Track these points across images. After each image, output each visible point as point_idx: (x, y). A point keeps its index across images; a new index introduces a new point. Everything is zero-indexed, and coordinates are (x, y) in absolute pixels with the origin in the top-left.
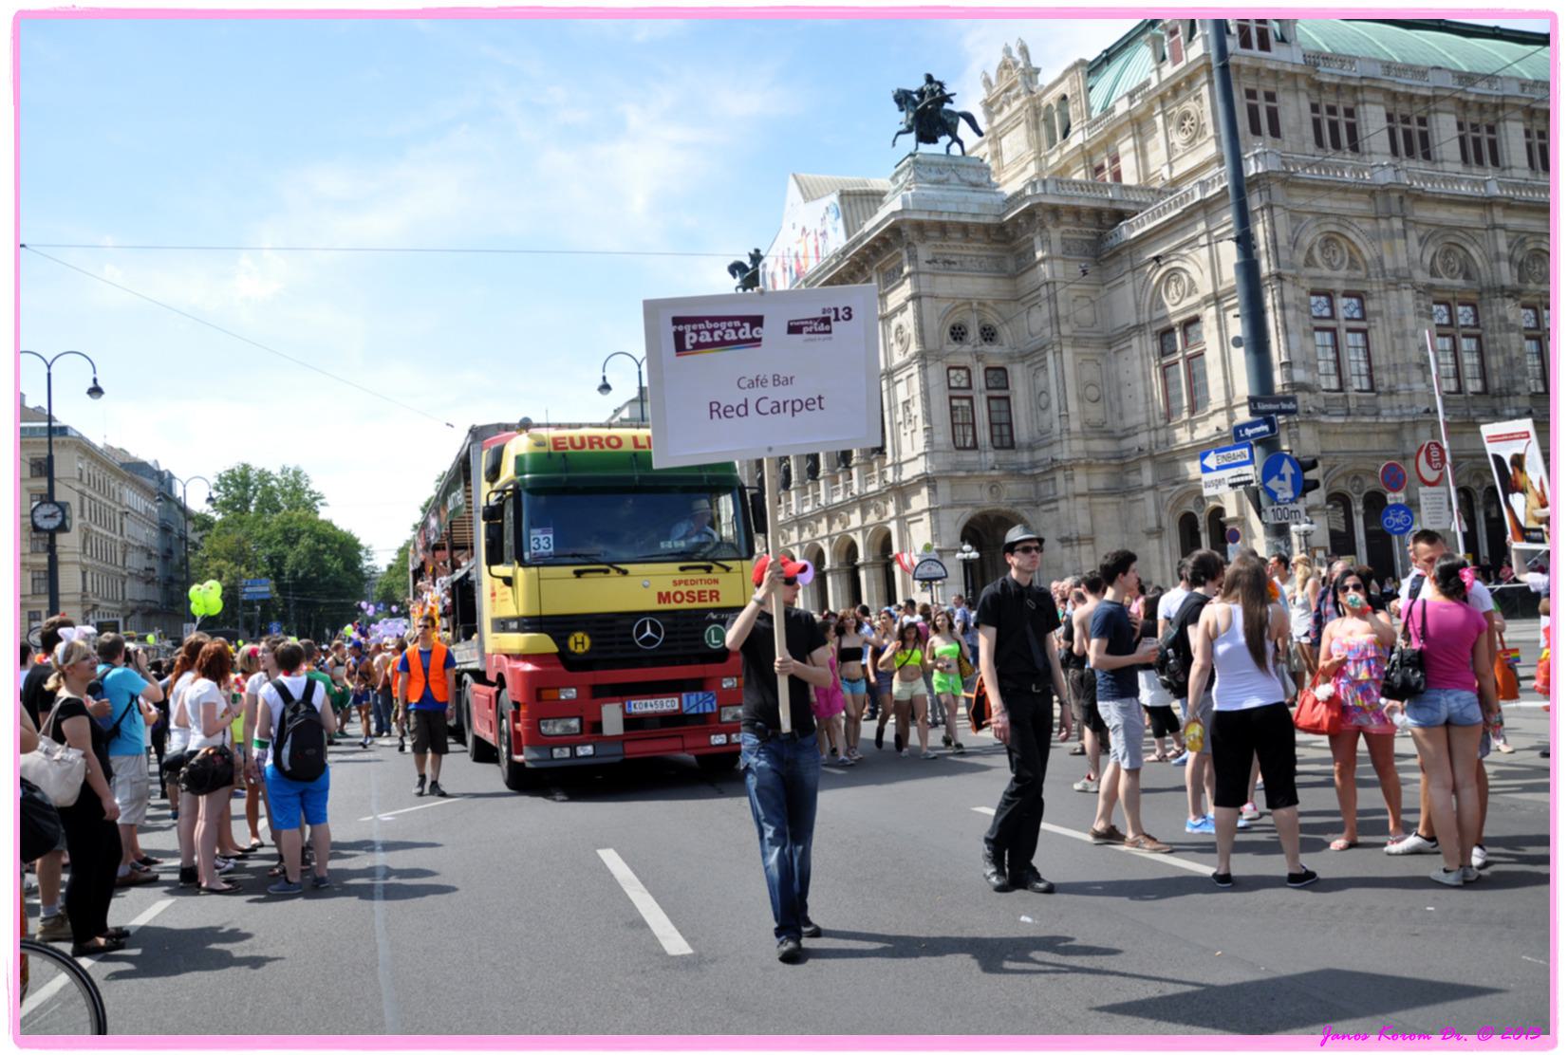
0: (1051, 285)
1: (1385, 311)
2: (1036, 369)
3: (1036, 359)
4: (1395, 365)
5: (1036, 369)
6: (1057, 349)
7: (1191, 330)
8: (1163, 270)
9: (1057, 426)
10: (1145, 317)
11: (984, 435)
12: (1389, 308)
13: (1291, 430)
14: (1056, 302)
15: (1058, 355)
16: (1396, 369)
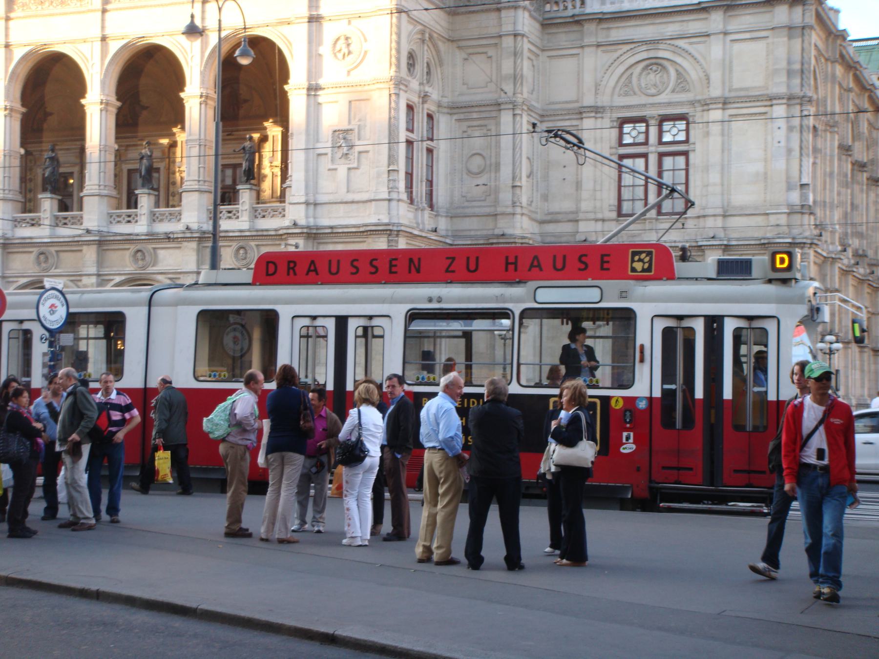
0: (519, 38)
1: (823, 151)
2: (469, 127)
3: (475, 116)
4: (825, 202)
5: (469, 127)
6: (518, 112)
7: (667, 126)
8: (645, 55)
9: (506, 196)
10: (604, 100)
11: (420, 189)
12: (826, 148)
13: (806, 250)
14: (522, 60)
15: (518, 118)
16: (825, 206)
